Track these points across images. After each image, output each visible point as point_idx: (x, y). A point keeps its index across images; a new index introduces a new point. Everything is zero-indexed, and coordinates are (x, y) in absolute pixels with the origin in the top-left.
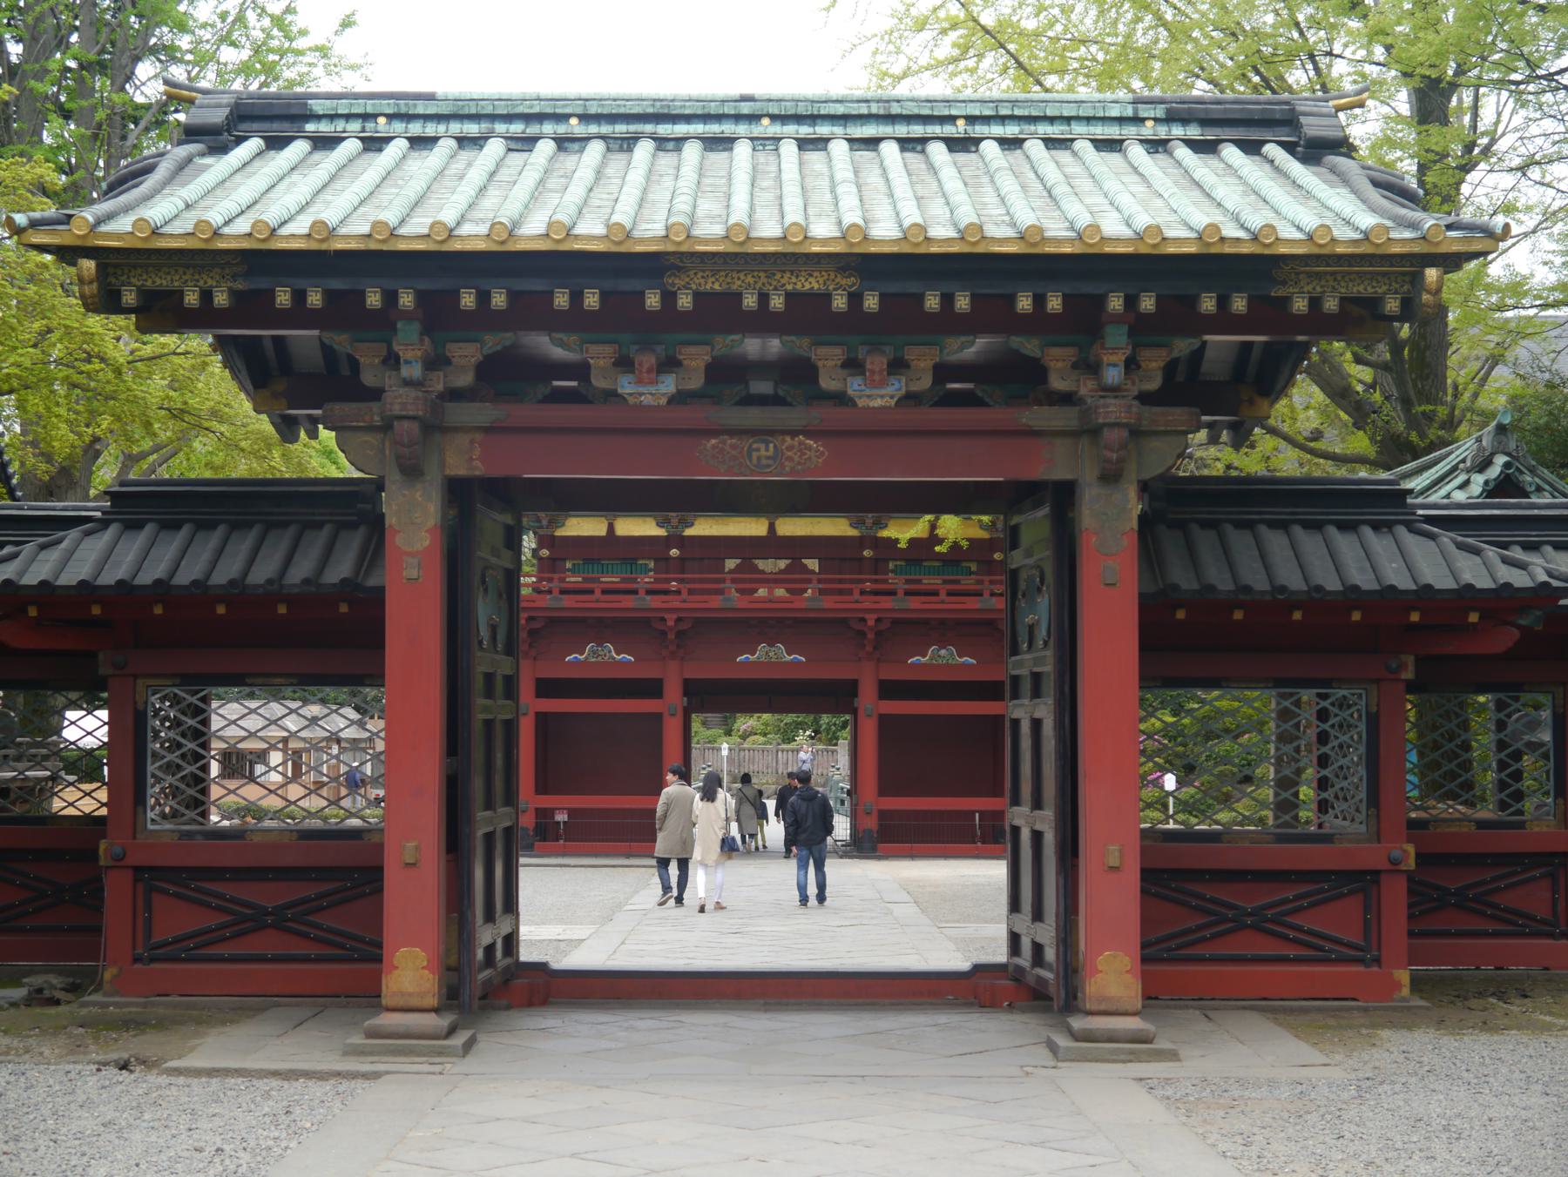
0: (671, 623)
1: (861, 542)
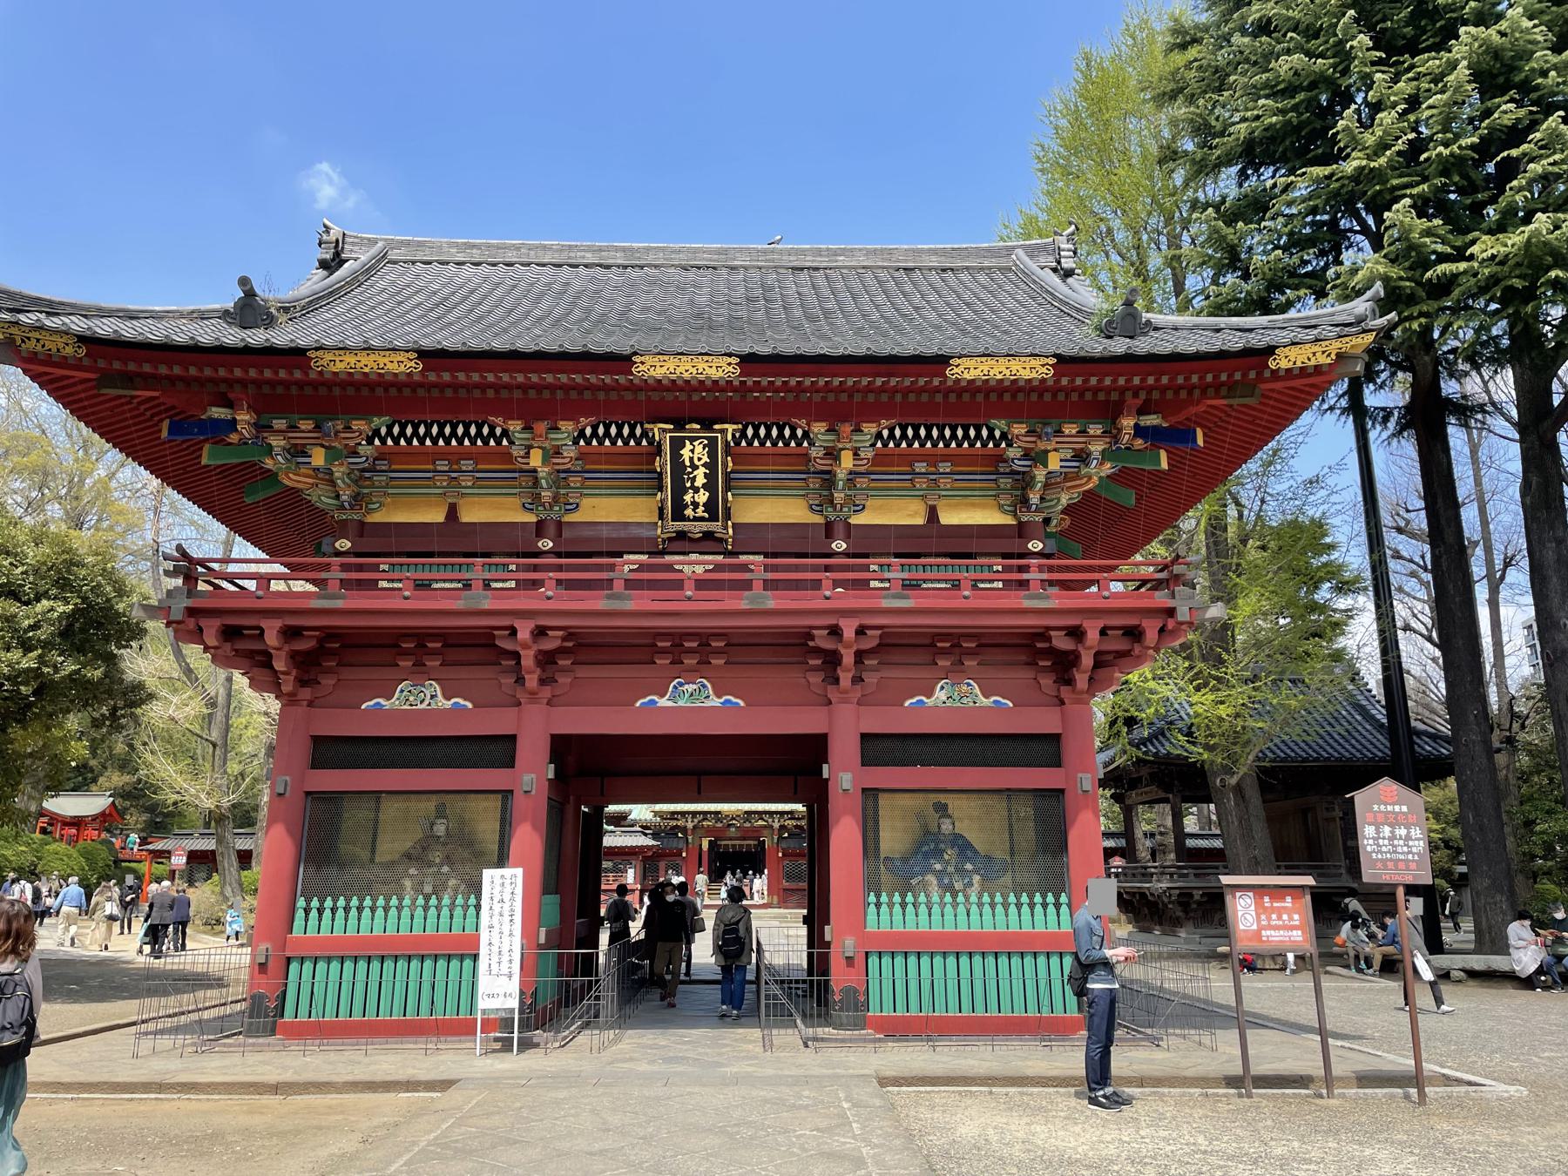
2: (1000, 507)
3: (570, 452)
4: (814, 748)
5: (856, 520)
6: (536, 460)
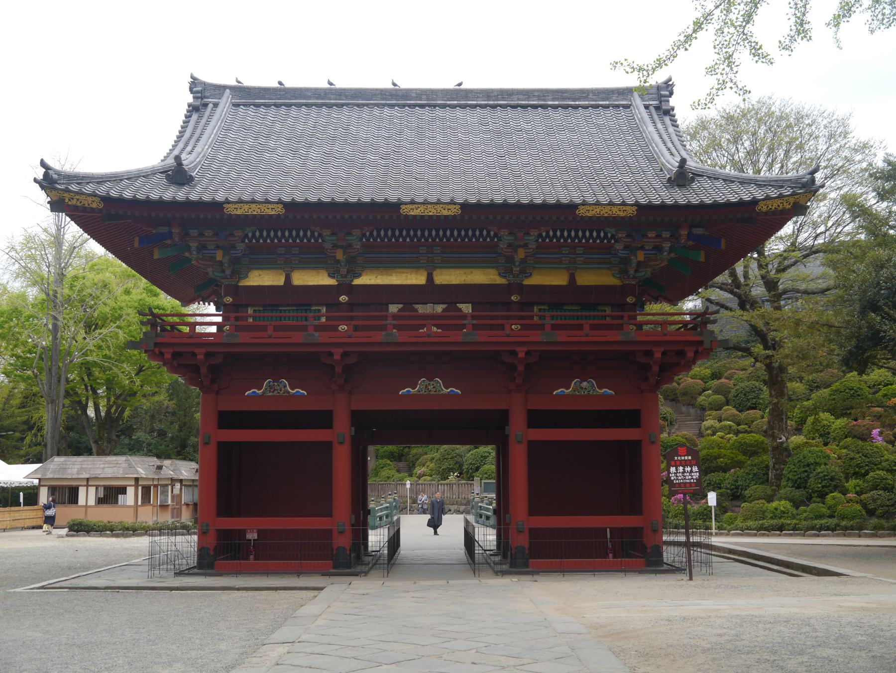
0: (337, 357)
1: (508, 289)
2: (613, 275)
3: (357, 245)
4: (502, 418)
5: (527, 282)
6: (340, 255)
